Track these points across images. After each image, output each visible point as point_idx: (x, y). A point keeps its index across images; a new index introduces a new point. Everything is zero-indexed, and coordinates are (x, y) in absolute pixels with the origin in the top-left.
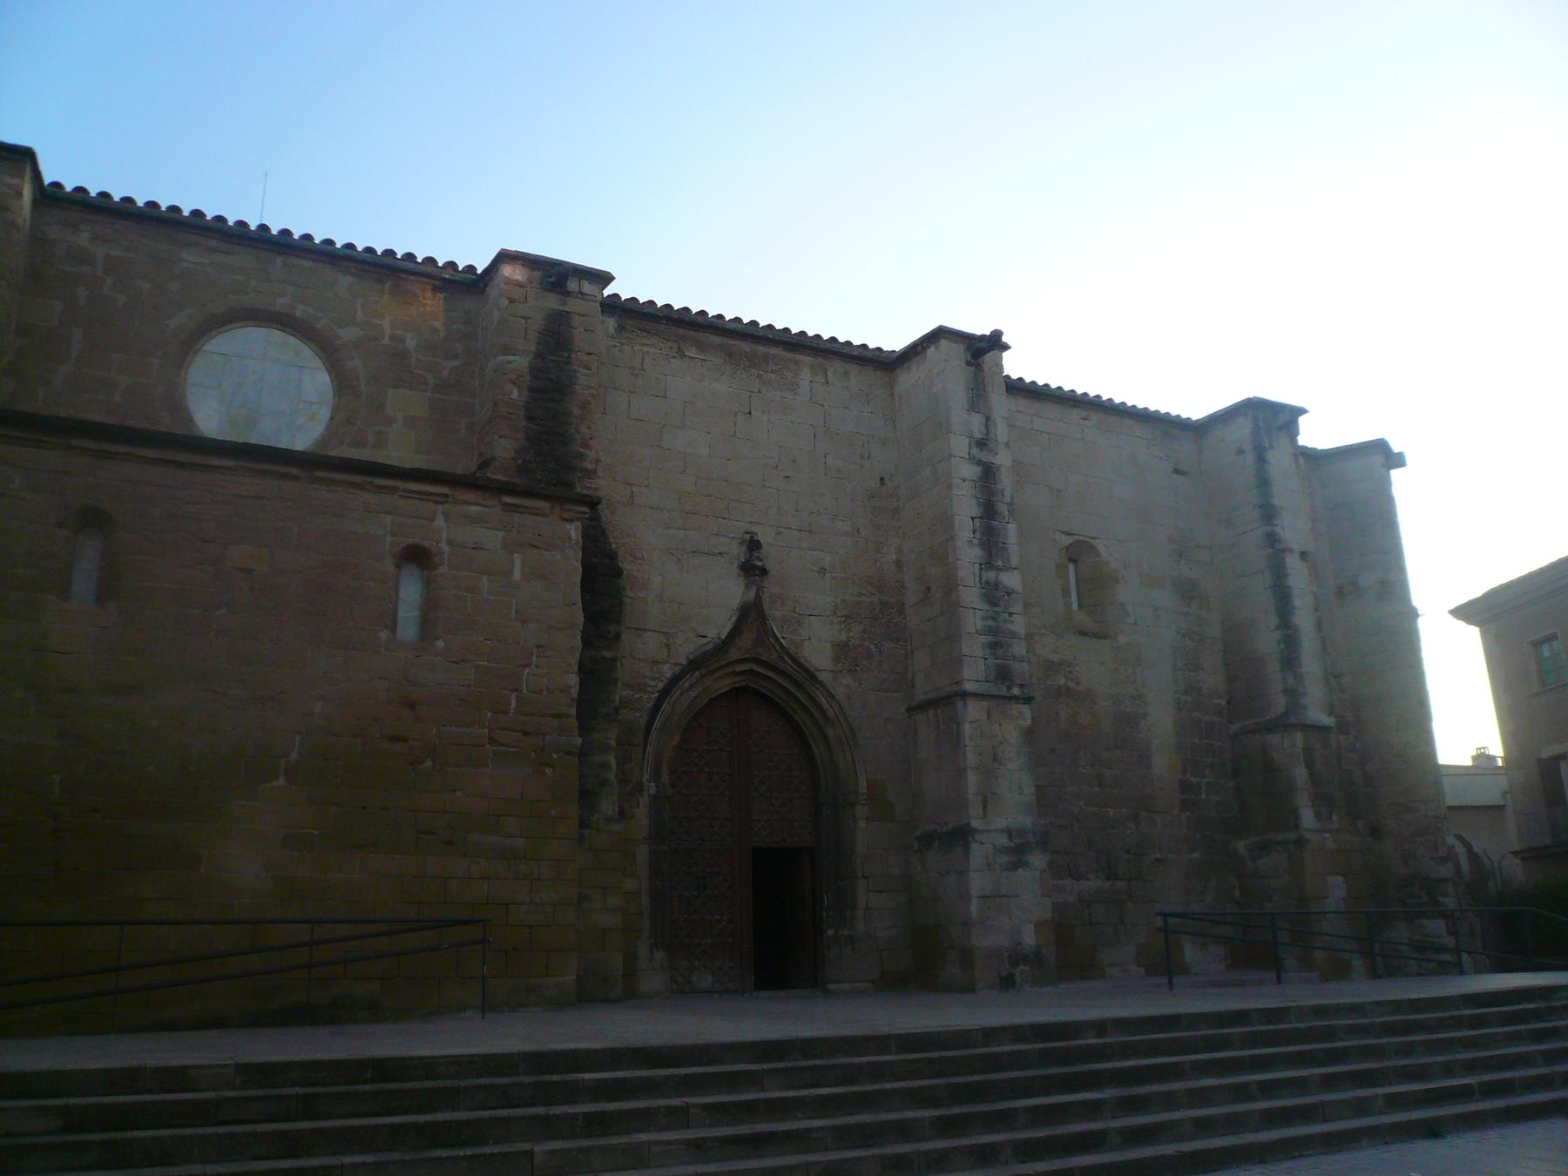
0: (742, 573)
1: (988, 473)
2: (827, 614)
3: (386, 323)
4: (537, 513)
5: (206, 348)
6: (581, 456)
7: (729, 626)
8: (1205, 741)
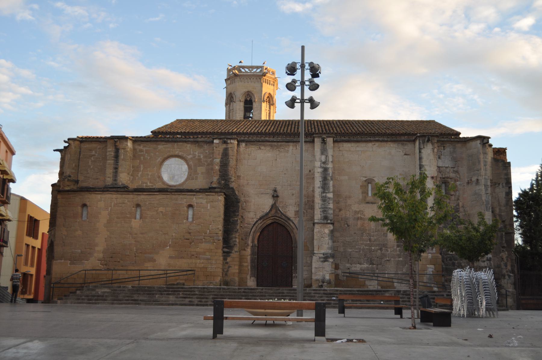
1: (325, 170)
3: (197, 153)
4: (213, 195)
5: (164, 164)
6: (231, 178)
7: (269, 209)
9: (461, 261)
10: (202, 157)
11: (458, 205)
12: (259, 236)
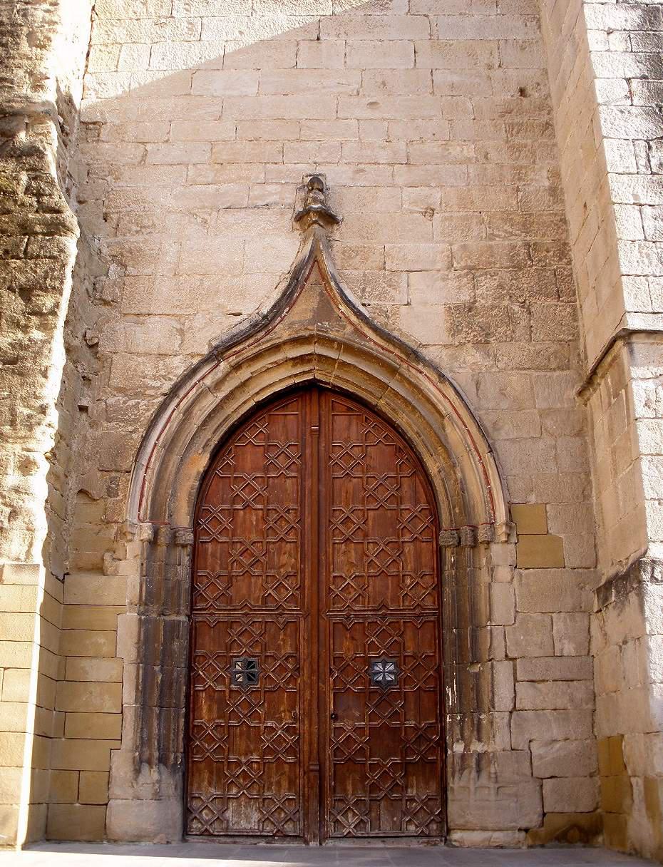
0: (297, 226)
2: (439, 266)
7: (276, 296)
12: (205, 476)
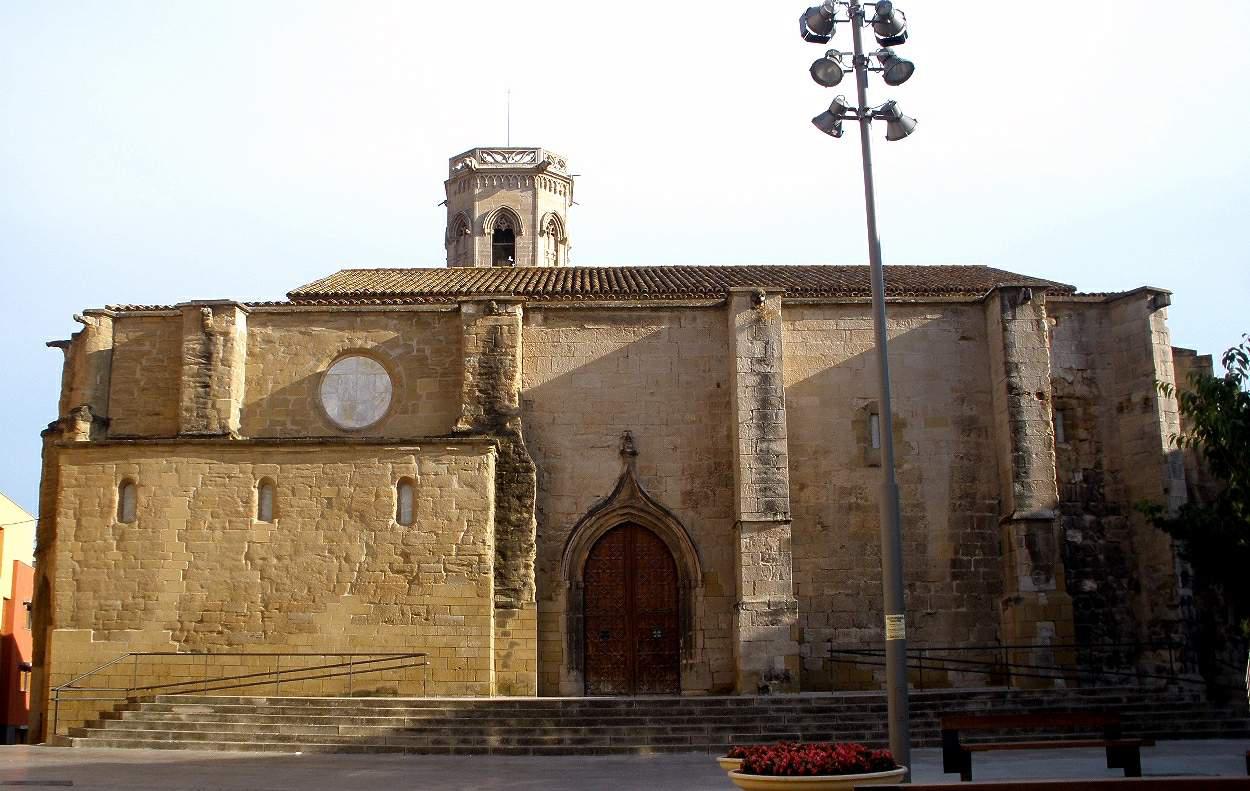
1: (765, 379)
3: (414, 343)
7: (613, 489)
8: (977, 531)
9: (1114, 609)
10: (428, 352)
11: (1098, 465)
12: (587, 561)
